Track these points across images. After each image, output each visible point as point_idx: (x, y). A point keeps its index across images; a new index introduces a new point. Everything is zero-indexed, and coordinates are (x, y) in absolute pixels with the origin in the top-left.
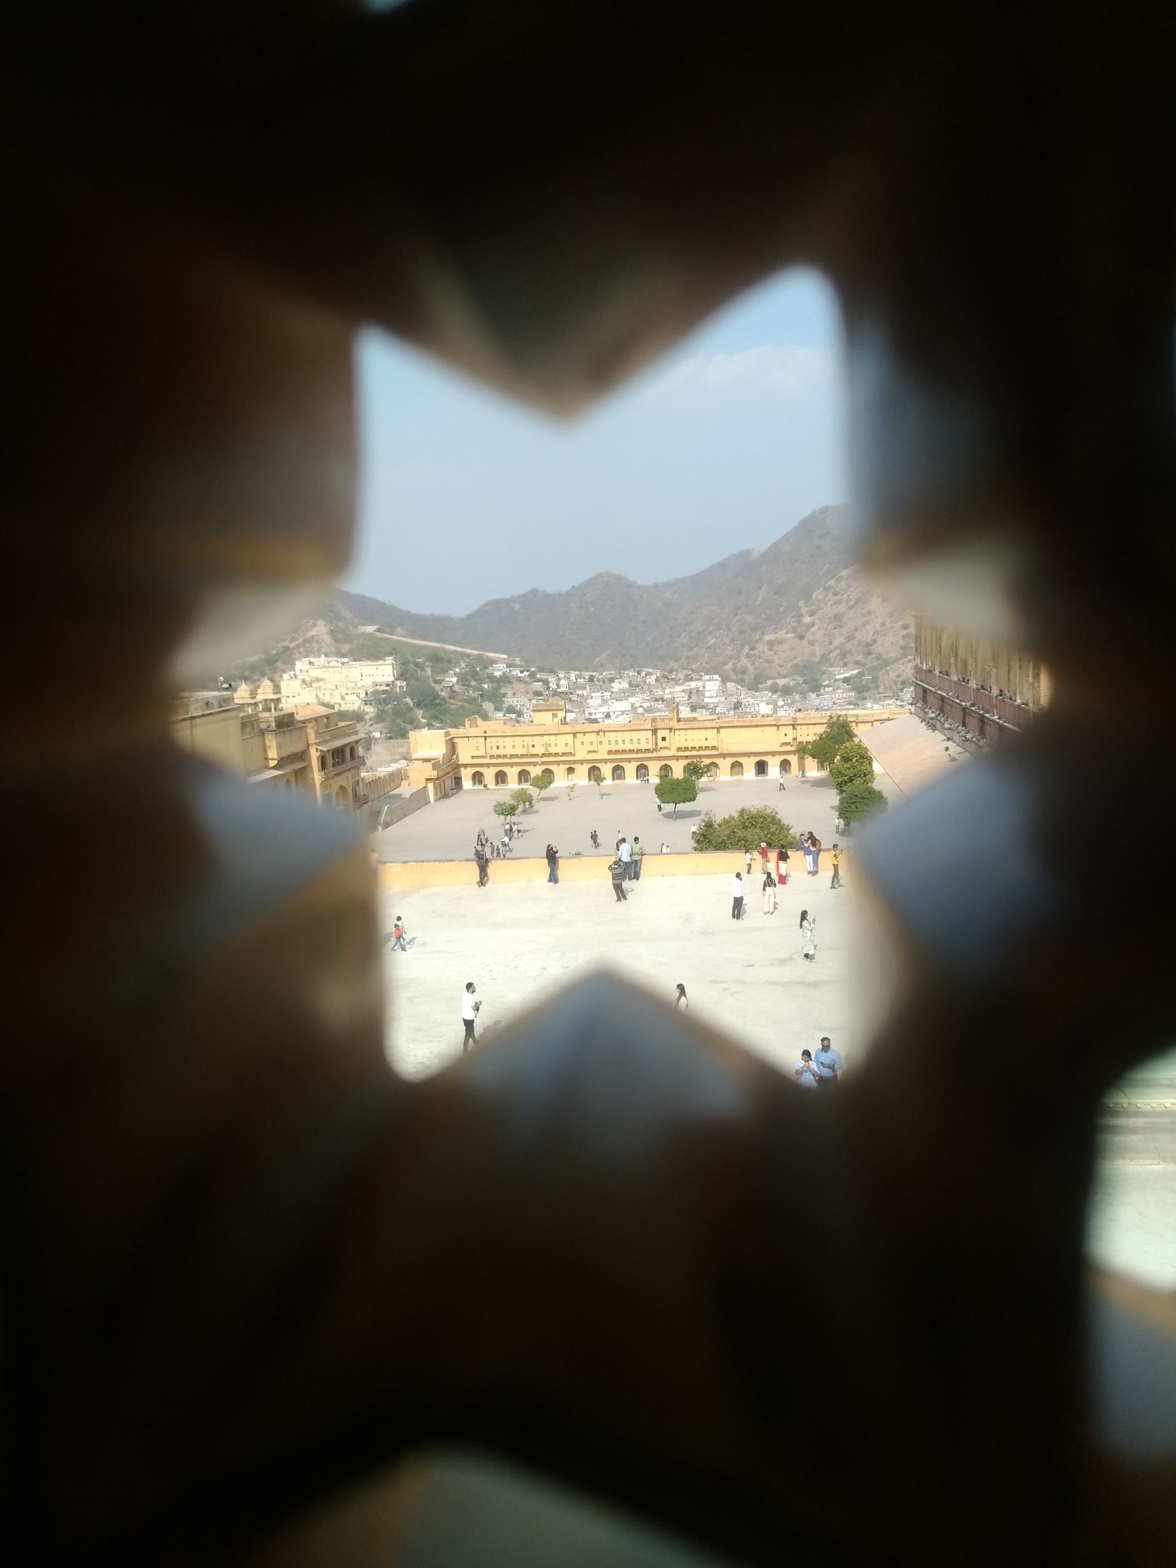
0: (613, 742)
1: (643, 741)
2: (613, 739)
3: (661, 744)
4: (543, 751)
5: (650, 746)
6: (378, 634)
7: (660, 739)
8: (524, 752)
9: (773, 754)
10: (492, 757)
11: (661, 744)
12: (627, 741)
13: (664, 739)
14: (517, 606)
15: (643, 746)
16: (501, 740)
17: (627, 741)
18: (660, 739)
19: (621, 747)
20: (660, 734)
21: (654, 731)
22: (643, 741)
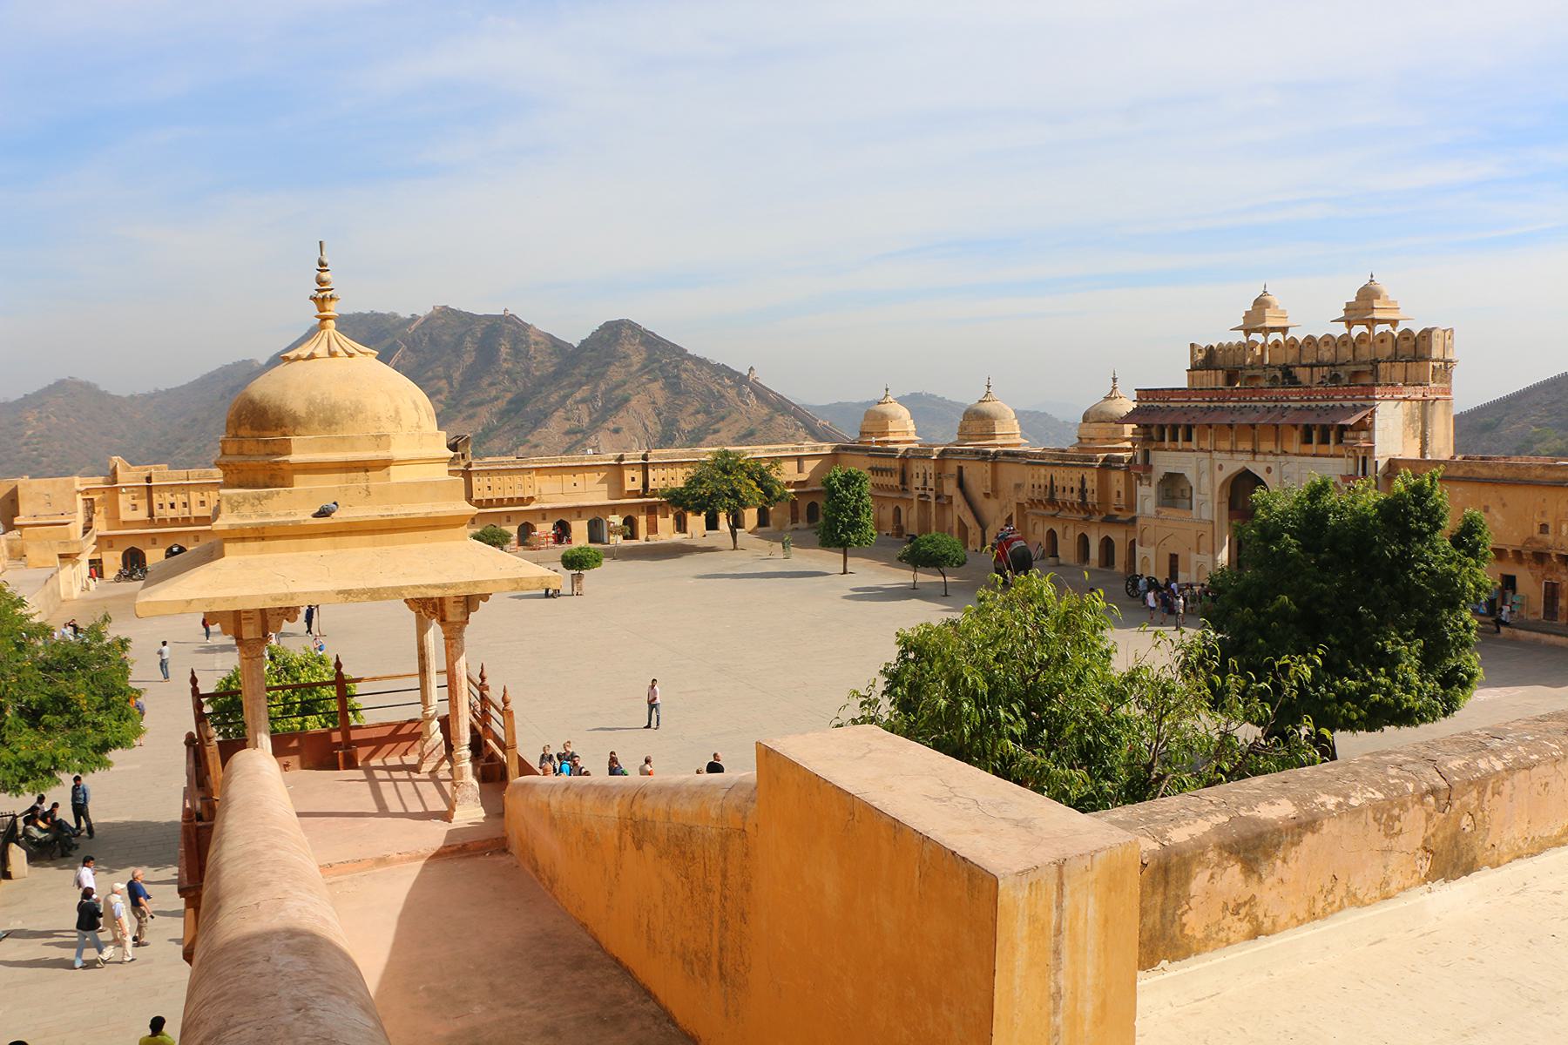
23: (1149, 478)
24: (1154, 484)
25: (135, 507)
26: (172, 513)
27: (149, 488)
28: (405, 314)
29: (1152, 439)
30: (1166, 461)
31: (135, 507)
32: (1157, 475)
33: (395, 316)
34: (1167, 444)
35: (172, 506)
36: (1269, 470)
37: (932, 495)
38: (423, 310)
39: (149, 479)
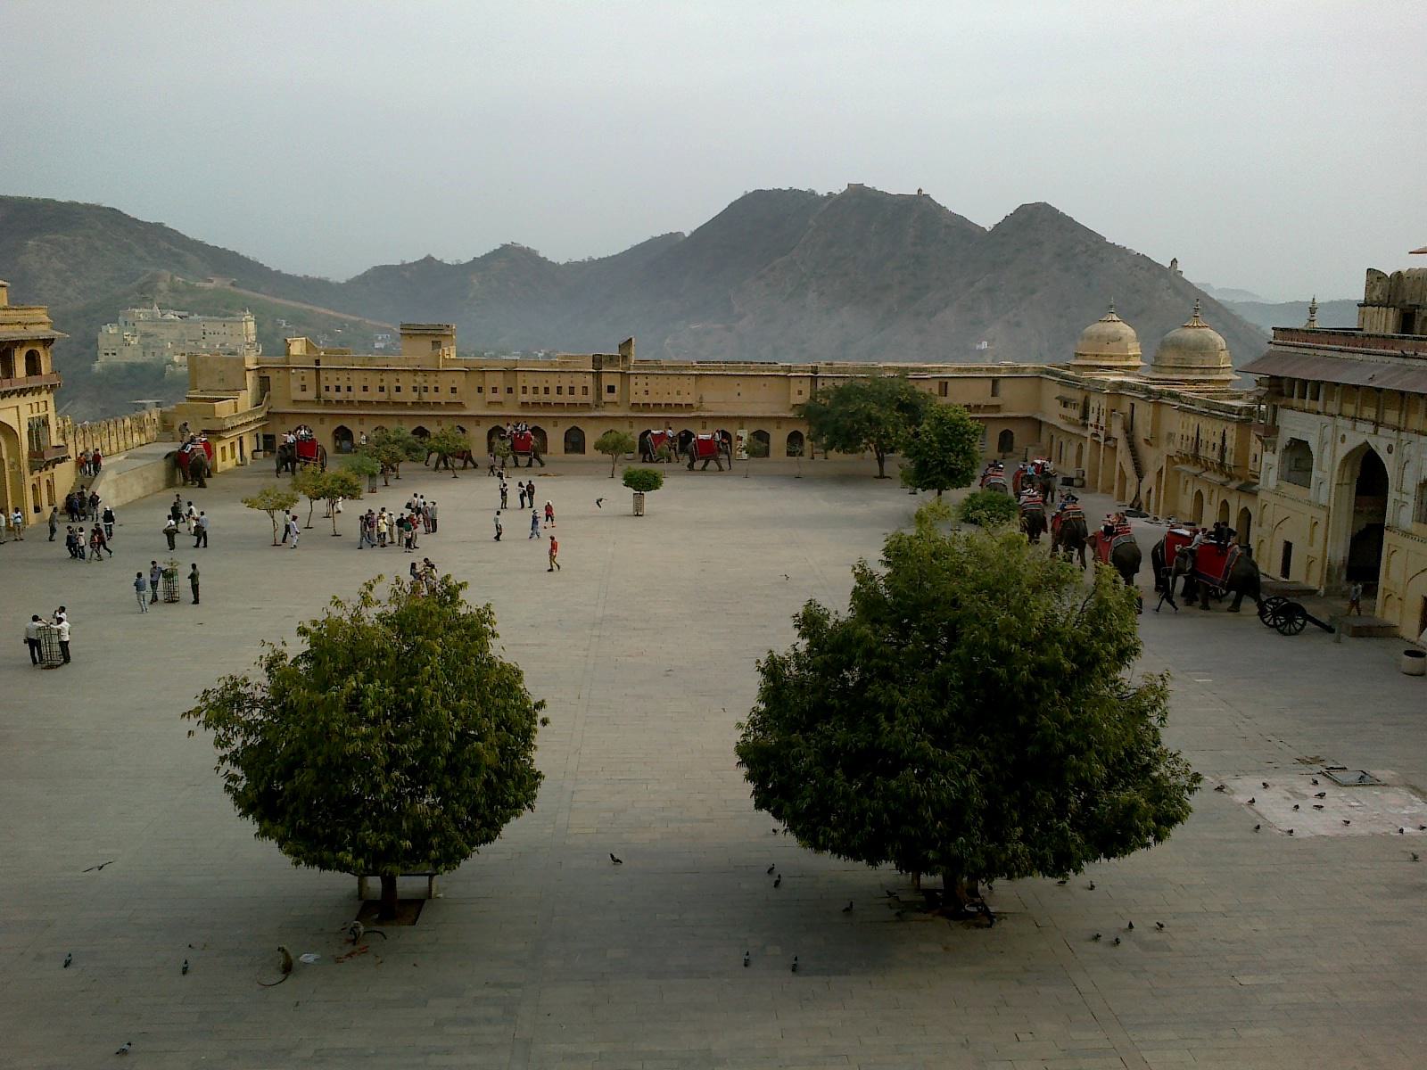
0: (530, 390)
1: (578, 391)
2: (530, 381)
3: (607, 397)
4: (414, 397)
5: (590, 398)
6: (232, 289)
7: (605, 389)
8: (383, 397)
9: (779, 420)
10: (328, 402)
11: (607, 397)
12: (553, 390)
13: (611, 389)
14: (407, 275)
15: (579, 398)
16: (343, 376)
17: (553, 390)
18: (605, 389)
19: (542, 397)
20: (607, 381)
21: (597, 375)
22: (578, 391)
23: (1274, 443)
24: (1279, 449)
25: (304, 389)
26: (338, 396)
27: (318, 370)
28: (822, 191)
29: (1280, 394)
30: (1294, 424)
31: (304, 389)
32: (1283, 439)
33: (813, 193)
34: (1295, 401)
35: (338, 389)
36: (1390, 449)
37: (1102, 434)
38: (839, 187)
39: (317, 362)
